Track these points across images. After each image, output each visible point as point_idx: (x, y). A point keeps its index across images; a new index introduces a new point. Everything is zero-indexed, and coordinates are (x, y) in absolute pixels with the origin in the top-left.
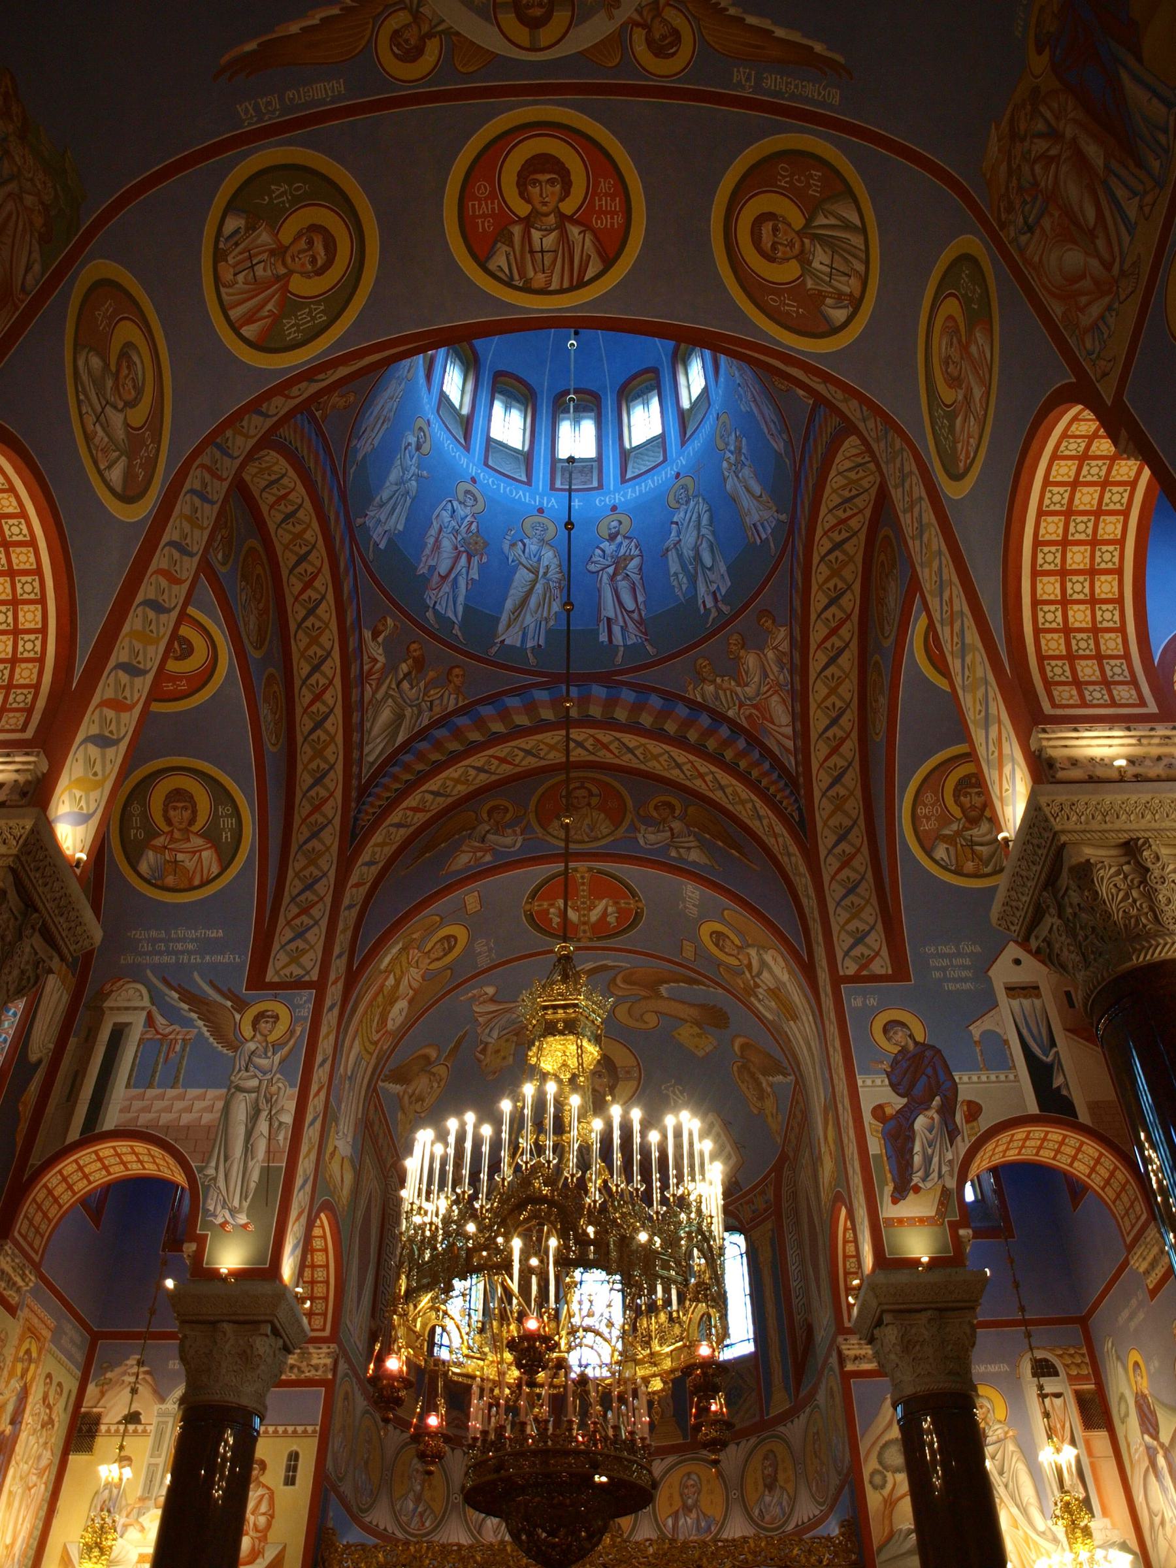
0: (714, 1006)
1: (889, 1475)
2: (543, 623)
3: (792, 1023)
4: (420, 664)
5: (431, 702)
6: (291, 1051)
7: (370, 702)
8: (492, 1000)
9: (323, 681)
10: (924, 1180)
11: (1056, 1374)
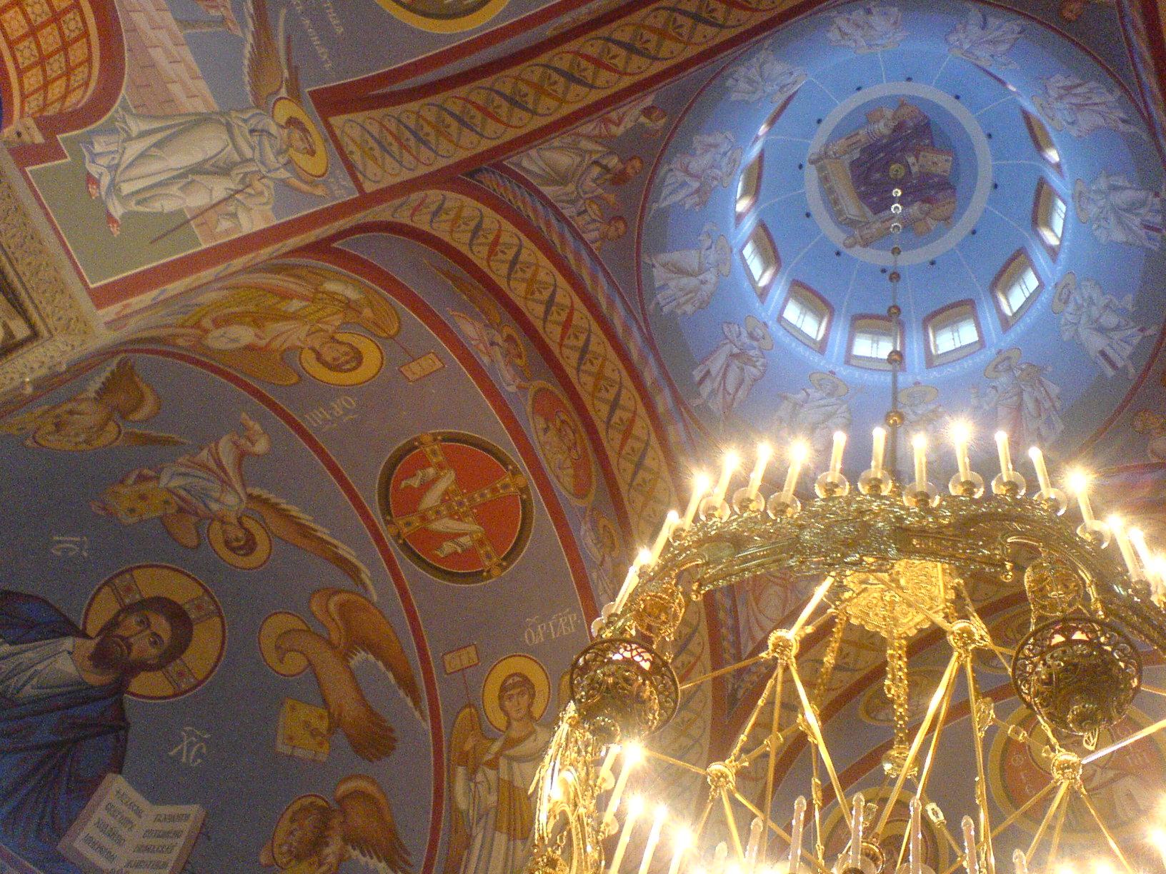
0: (391, 730)
2: (674, 303)
3: (504, 837)
4: (619, 179)
5: (585, 211)
6: (297, 189)
8: (242, 455)
9: (619, 63)
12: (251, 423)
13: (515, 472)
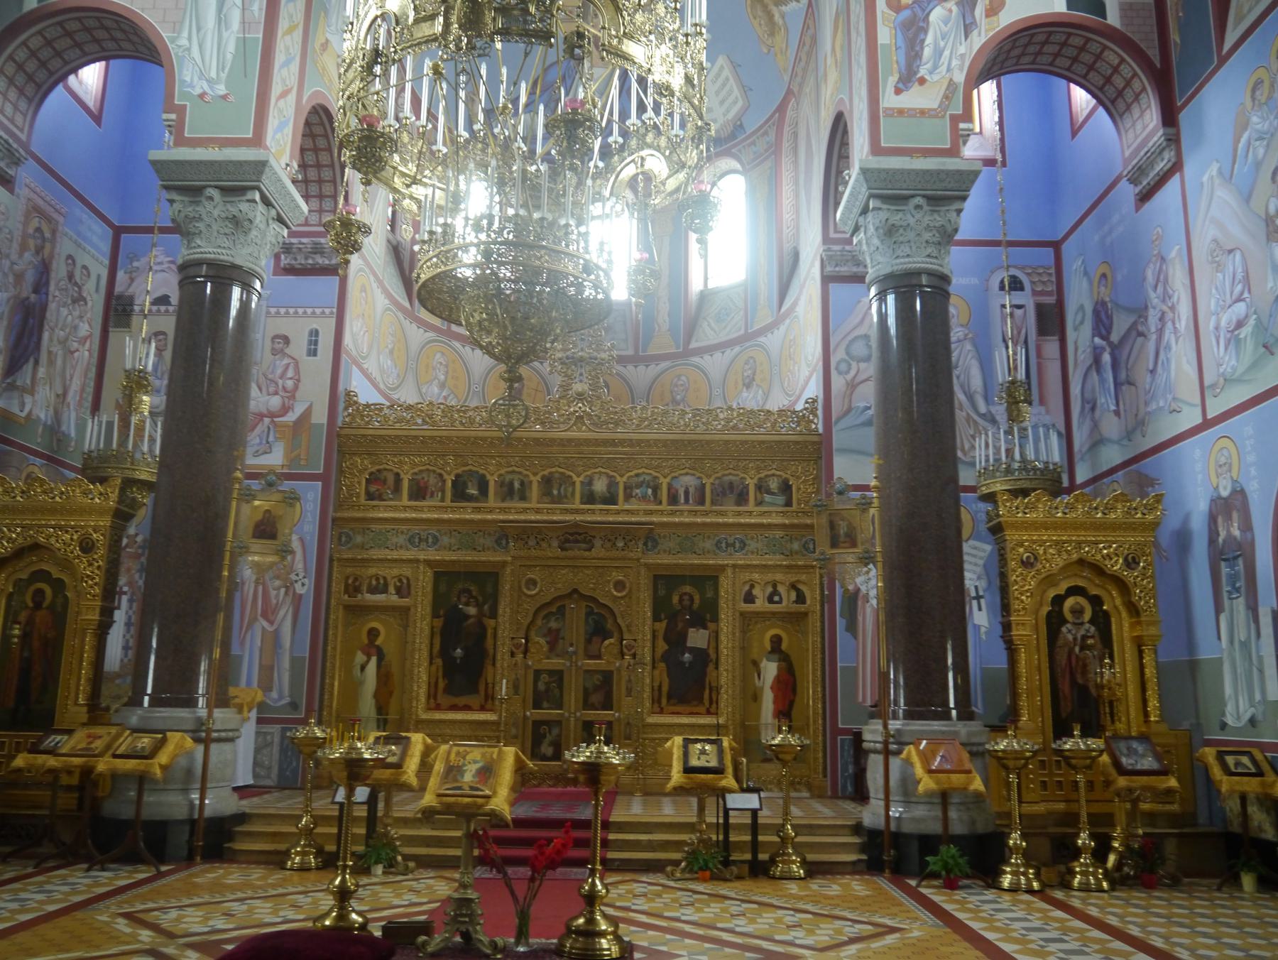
1: (854, 364)
10: (931, 73)
11: (1022, 289)
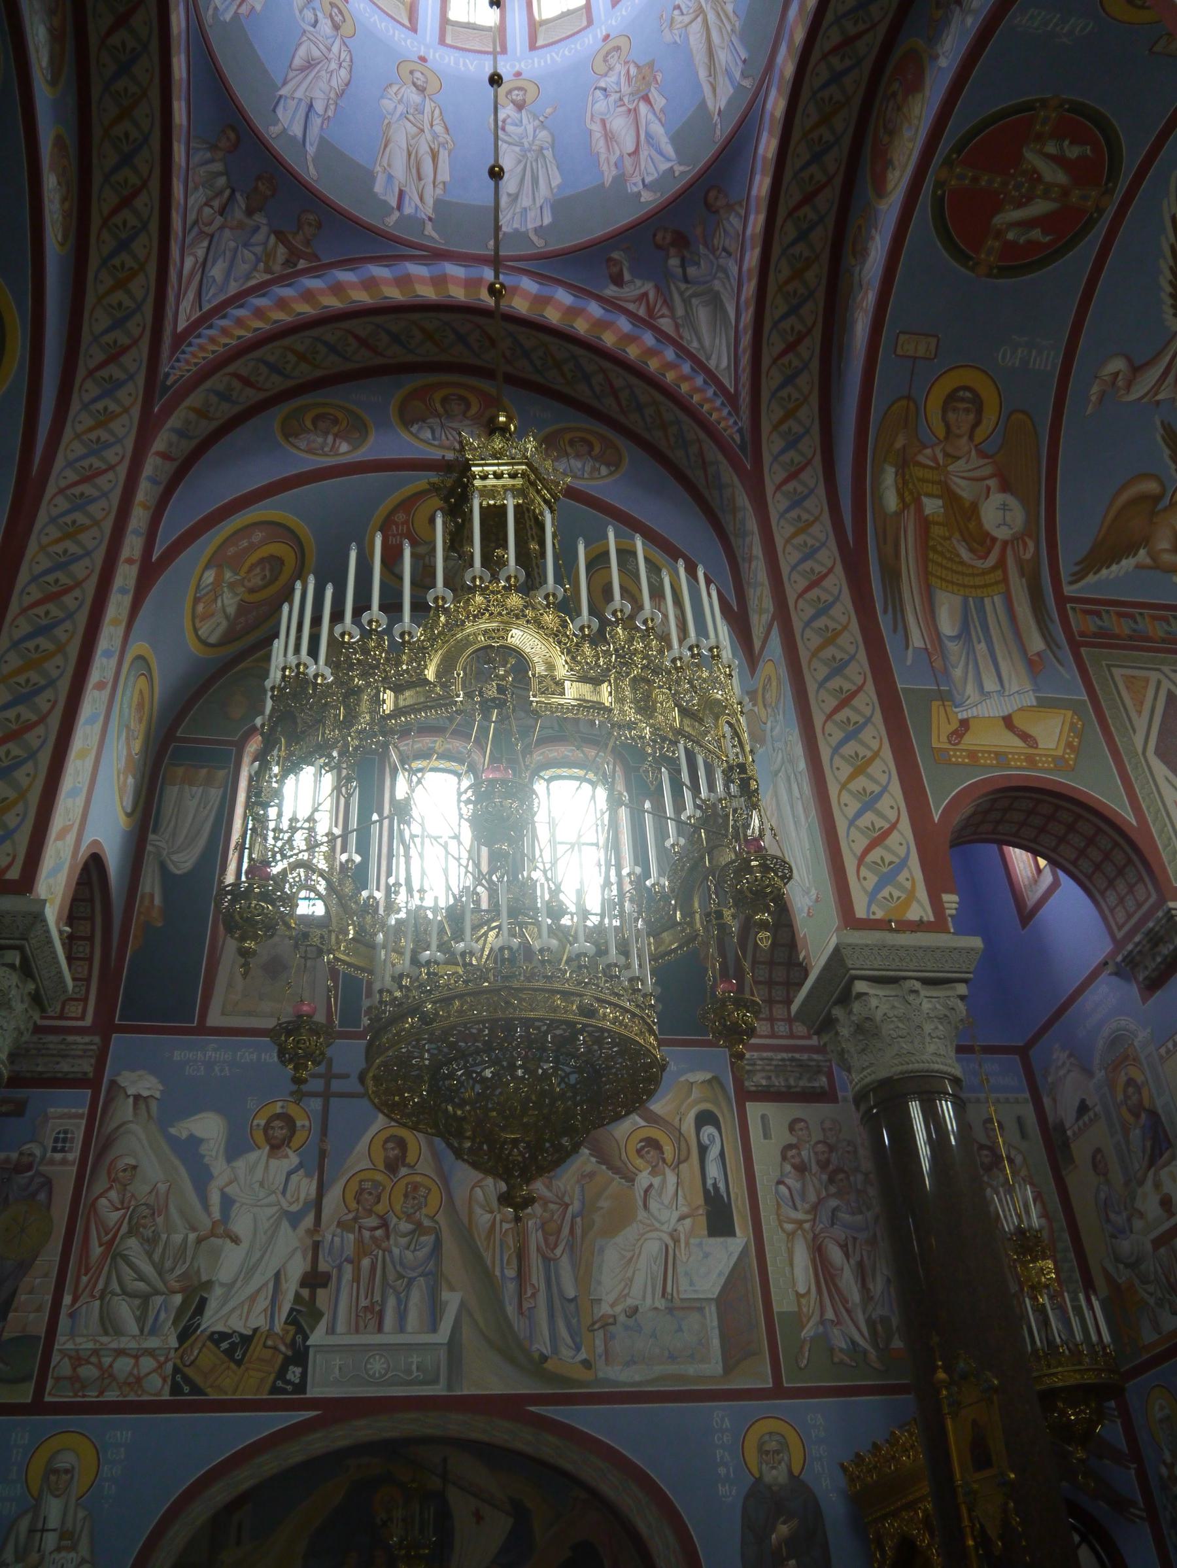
7: (677, 326)
8: (1136, 369)
12: (1093, 398)
13: (939, 184)
